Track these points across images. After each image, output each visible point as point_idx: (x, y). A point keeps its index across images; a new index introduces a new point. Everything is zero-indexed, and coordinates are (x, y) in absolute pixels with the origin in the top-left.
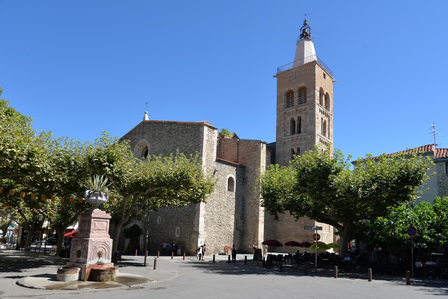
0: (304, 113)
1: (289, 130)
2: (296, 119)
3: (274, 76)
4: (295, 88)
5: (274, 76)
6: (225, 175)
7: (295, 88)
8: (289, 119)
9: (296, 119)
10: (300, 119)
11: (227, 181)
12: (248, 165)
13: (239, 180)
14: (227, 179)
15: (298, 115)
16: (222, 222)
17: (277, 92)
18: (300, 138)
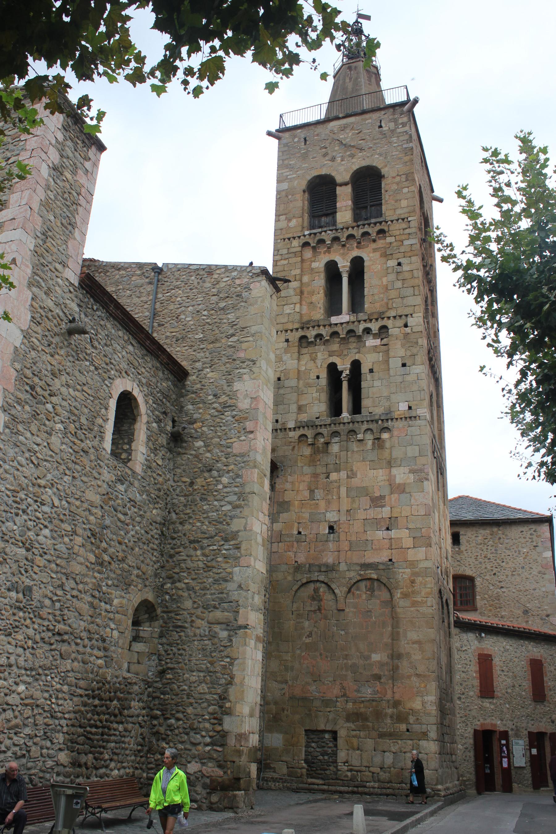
0: (375, 250)
1: (320, 298)
2: (344, 265)
3: (269, 134)
4: (342, 172)
5: (269, 134)
6: (106, 373)
7: (342, 172)
8: (319, 264)
9: (344, 265)
10: (358, 266)
11: (113, 404)
12: (198, 365)
13: (159, 421)
14: (116, 396)
15: (356, 253)
16: (72, 617)
17: (280, 181)
18: (362, 326)
